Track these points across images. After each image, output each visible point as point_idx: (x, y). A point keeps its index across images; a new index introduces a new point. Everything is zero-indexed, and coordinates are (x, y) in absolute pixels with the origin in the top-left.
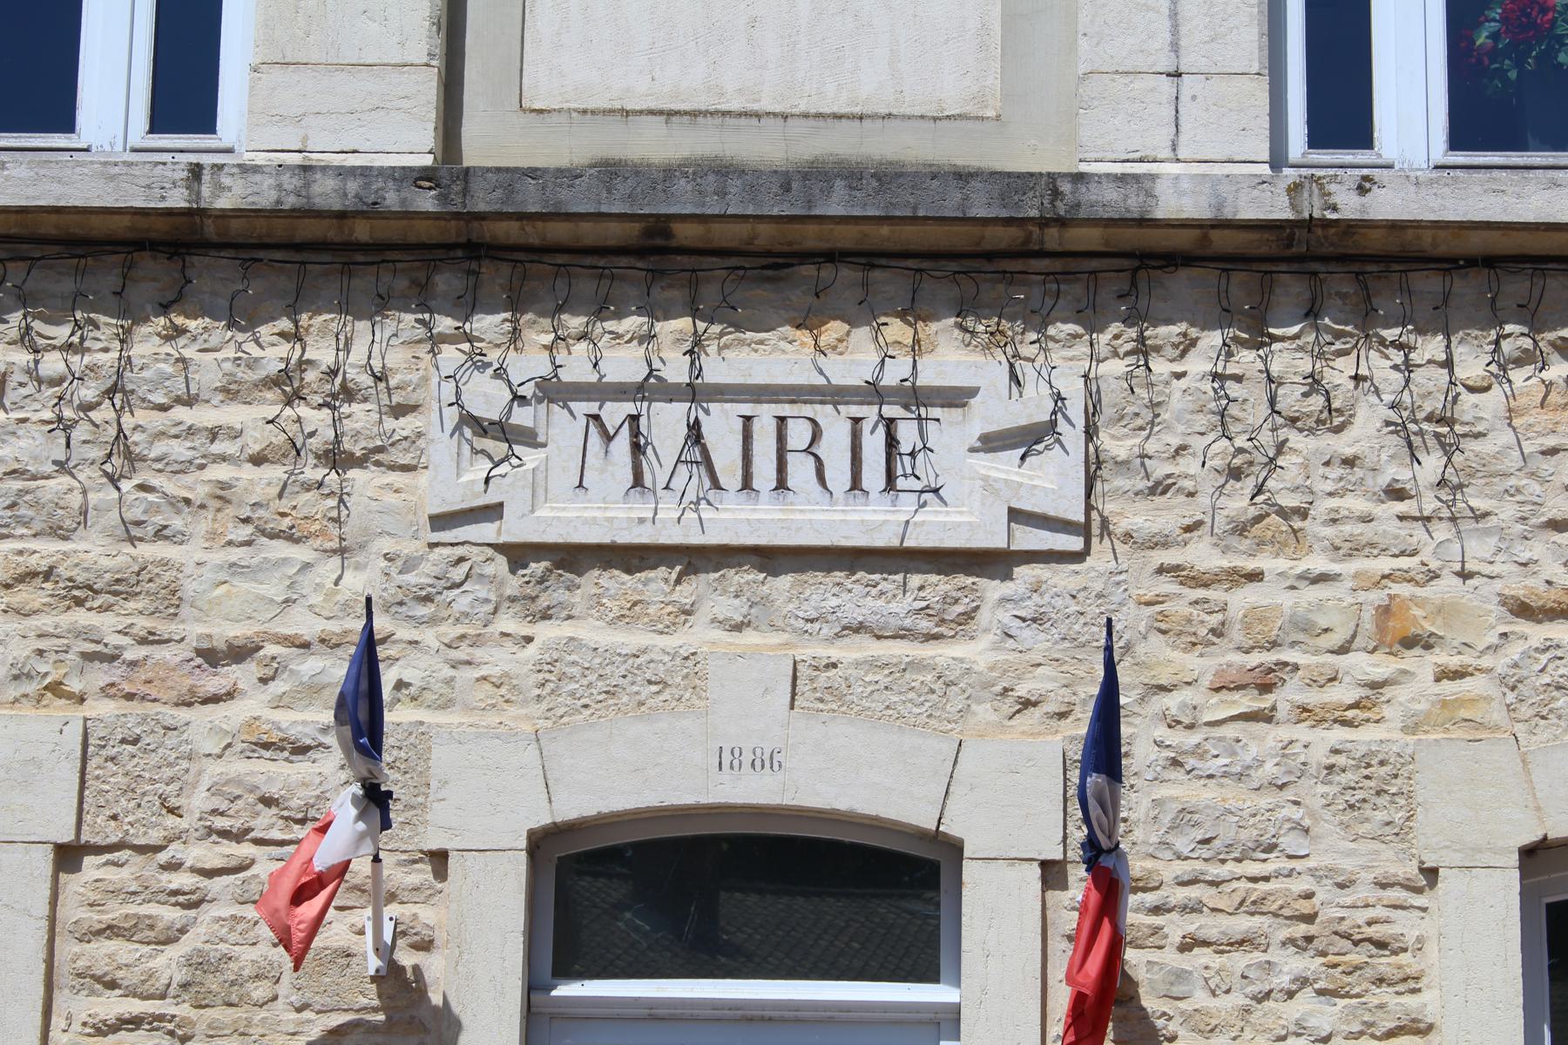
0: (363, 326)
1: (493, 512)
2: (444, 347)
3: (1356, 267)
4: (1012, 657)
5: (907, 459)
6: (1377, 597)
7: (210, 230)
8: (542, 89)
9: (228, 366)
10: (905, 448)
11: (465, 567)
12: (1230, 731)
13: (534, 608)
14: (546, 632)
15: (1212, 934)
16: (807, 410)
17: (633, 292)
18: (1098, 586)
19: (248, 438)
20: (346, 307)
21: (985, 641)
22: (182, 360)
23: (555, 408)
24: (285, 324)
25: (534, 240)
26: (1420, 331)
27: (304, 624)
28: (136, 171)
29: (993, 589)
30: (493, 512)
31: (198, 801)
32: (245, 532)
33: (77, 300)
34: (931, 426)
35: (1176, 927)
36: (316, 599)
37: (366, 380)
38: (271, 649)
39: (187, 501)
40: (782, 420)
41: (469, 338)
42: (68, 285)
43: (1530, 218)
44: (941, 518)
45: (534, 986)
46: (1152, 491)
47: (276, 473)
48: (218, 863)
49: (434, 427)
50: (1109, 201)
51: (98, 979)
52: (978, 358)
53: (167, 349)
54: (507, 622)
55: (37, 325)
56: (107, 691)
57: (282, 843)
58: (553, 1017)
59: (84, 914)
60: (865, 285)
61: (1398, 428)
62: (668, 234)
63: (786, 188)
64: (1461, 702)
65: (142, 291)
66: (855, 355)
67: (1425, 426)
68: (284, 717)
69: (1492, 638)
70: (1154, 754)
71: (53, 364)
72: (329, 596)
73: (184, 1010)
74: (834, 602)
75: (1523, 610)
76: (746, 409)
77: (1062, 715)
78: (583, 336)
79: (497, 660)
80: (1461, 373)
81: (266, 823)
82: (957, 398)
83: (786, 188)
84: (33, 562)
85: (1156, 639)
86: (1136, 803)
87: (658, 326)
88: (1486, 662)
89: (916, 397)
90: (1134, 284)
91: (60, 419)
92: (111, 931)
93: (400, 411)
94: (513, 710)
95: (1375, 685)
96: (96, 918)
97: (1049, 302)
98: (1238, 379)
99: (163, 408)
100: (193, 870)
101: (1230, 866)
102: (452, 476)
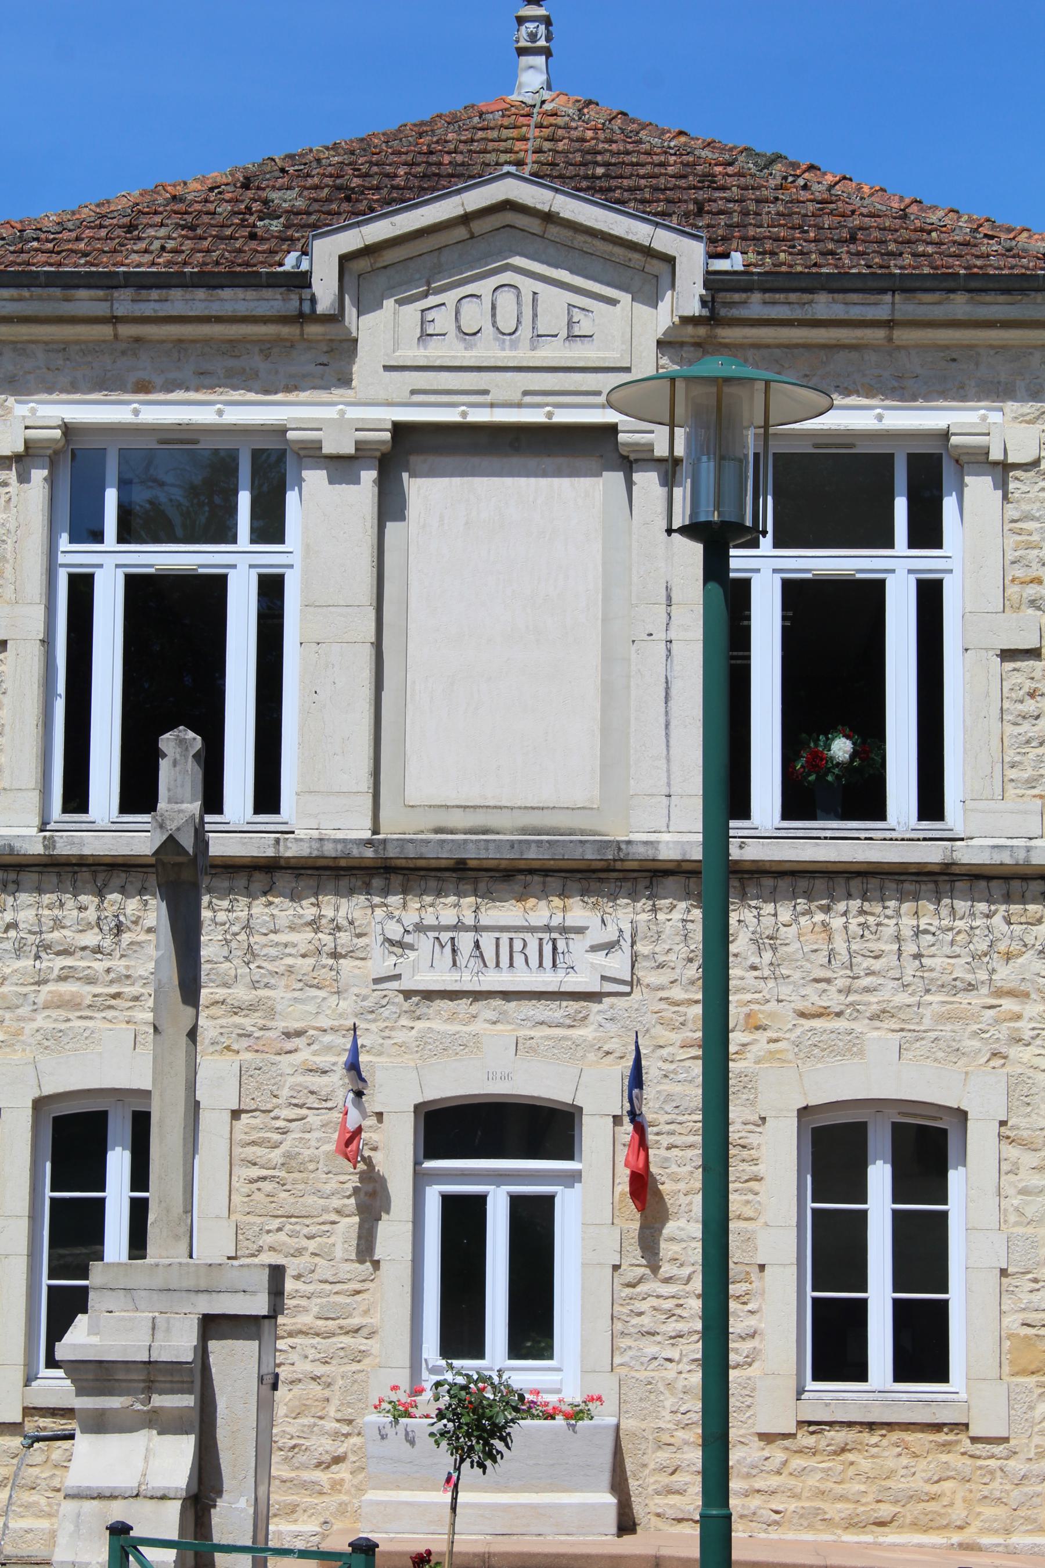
0: (344, 901)
1: (397, 977)
2: (376, 909)
3: (739, 876)
4: (602, 1034)
5: (561, 956)
6: (745, 1010)
7: (282, 863)
8: (413, 796)
9: (291, 917)
10: (560, 950)
11: (387, 999)
12: (687, 1063)
13: (414, 1015)
14: (419, 1025)
15: (679, 1143)
16: (521, 935)
17: (451, 886)
18: (636, 1006)
19: (299, 947)
20: (337, 893)
21: (592, 1028)
22: (272, 915)
23: (421, 934)
24: (313, 900)
25: (411, 866)
26: (765, 902)
27: (326, 1023)
28: (253, 841)
29: (595, 1007)
30: (397, 977)
31: (285, 1093)
32: (300, 985)
33: (231, 890)
34: (571, 941)
35: (665, 1140)
36: (329, 1012)
37: (345, 923)
38: (311, 1032)
39: (277, 973)
40: (511, 939)
41: (386, 905)
42: (226, 884)
43: (808, 859)
44: (574, 979)
45: (417, 1163)
46: (658, 967)
47: (311, 961)
48: (294, 1117)
49: (373, 941)
50: (641, 852)
51: (249, 1162)
52: (588, 914)
53: (266, 910)
54: (404, 1021)
55: (214, 900)
56: (248, 1049)
57: (318, 1109)
58: (424, 1174)
59: (243, 1136)
60: (544, 883)
61: (754, 941)
62: (465, 864)
63: (512, 847)
64: (777, 1052)
65: (256, 886)
66: (541, 912)
67: (766, 941)
68: (317, 1059)
69: (790, 1026)
70: (658, 1073)
71: (222, 916)
72: (334, 1011)
73: (283, 1174)
74: (532, 1013)
75: (802, 1015)
76: (497, 935)
77: (621, 1058)
78: (432, 905)
79: (400, 1036)
80: (780, 918)
81: (312, 1101)
82: (580, 930)
83: (512, 847)
84: (217, 997)
85: (659, 1027)
86: (649, 1091)
87: (462, 900)
88: (787, 1036)
89: (564, 930)
90: (651, 883)
91: (225, 939)
92: (253, 1143)
93: (359, 936)
94: (407, 1056)
95: (744, 1045)
96: (248, 1138)
97: (618, 890)
98: (692, 921)
99: (266, 935)
100: (284, 1120)
101: (686, 1116)
102: (382, 962)
